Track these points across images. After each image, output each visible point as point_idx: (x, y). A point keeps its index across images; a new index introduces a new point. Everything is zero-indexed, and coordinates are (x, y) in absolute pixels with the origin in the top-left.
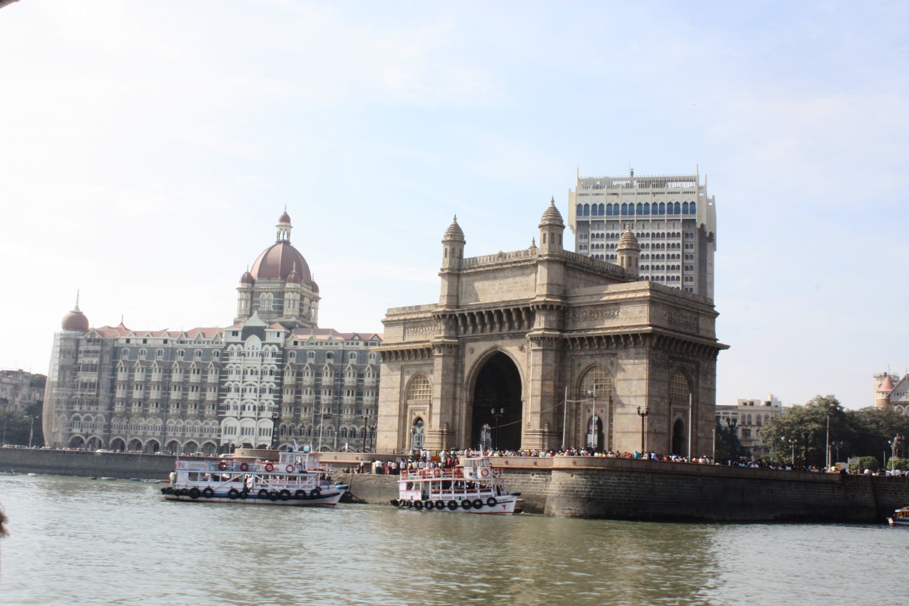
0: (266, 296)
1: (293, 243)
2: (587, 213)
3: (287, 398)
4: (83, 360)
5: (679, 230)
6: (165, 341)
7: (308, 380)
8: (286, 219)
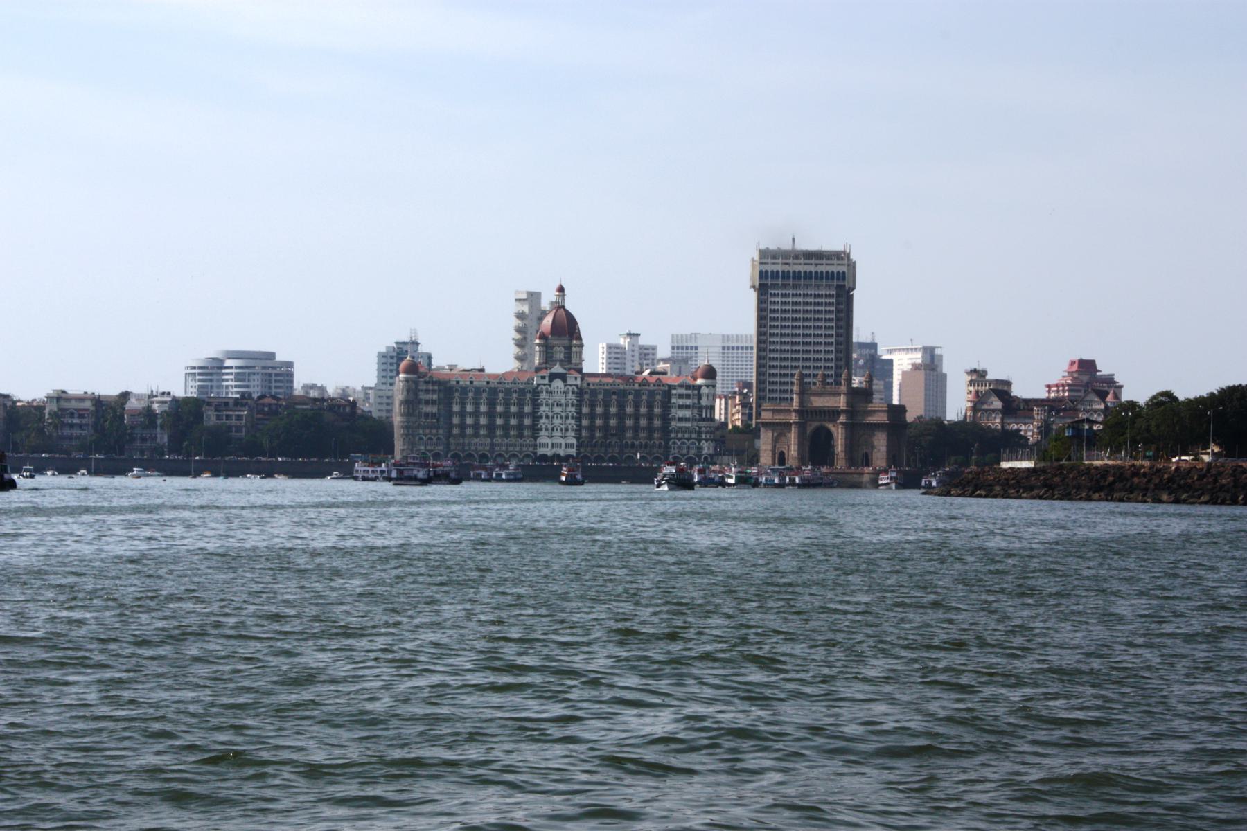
0: (558, 349)
1: (567, 308)
2: (767, 278)
3: (585, 423)
4: (422, 396)
5: (833, 292)
6: (488, 383)
7: (599, 410)
8: (561, 289)
